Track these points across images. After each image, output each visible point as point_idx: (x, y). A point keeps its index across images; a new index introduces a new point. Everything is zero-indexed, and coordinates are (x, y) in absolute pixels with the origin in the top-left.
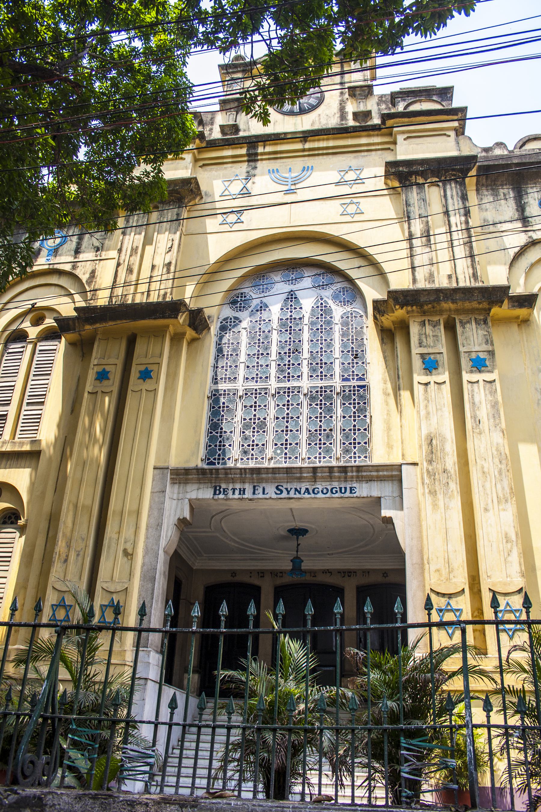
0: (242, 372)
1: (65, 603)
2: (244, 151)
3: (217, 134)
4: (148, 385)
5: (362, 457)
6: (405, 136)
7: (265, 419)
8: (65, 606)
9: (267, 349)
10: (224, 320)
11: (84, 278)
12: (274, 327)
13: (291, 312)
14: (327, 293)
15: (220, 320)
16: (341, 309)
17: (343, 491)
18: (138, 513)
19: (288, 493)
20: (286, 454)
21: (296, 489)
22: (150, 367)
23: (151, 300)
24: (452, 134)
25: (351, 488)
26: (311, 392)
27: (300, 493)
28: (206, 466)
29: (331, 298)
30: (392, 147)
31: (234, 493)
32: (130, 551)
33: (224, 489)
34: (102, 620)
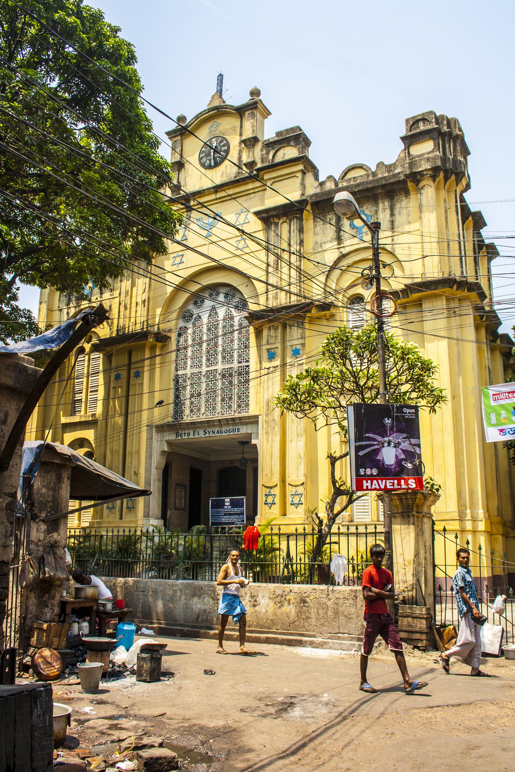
4: (138, 381)
18: (138, 452)
24: (299, 175)
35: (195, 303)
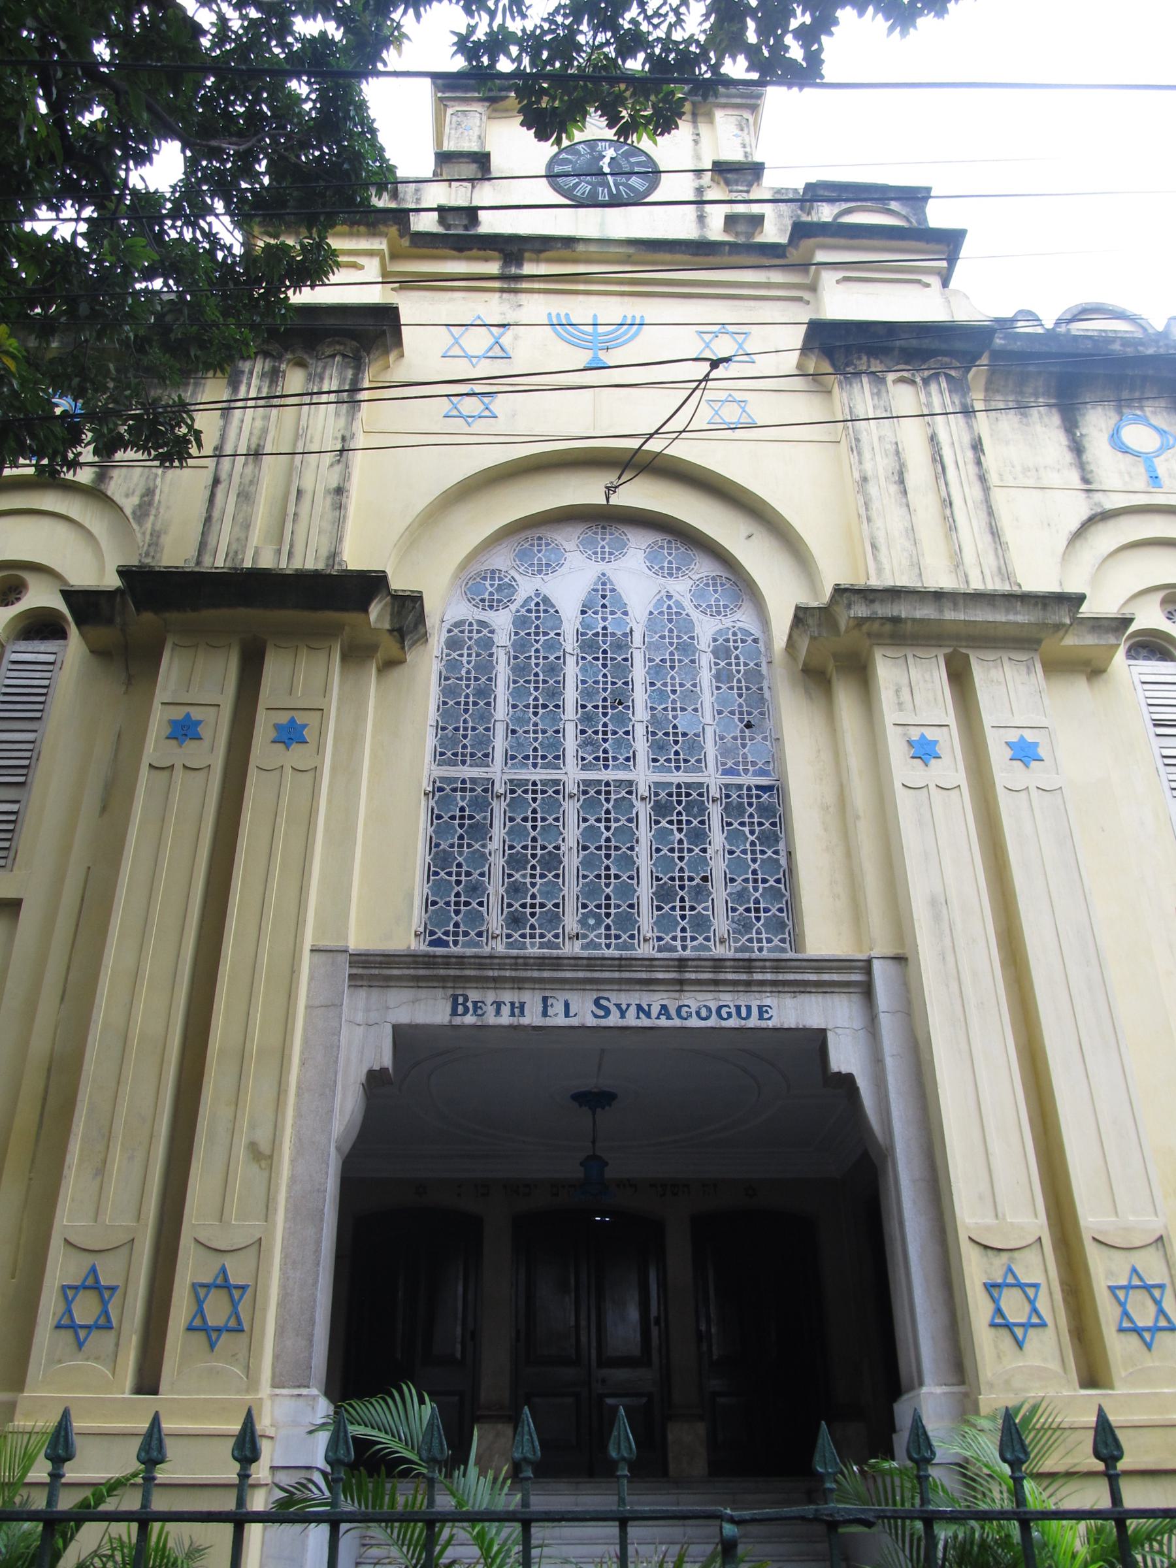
0: (500, 744)
1: (97, 1280)
2: (494, 268)
3: (426, 223)
4: (297, 755)
5: (776, 941)
6: (840, 275)
7: (557, 848)
8: (97, 1288)
9: (553, 694)
10: (457, 625)
11: (129, 505)
12: (569, 649)
13: (604, 619)
14: (680, 588)
15: (446, 626)
16: (712, 619)
17: (744, 1013)
19: (623, 1016)
20: (608, 928)
21: (639, 1008)
22: (300, 719)
23: (297, 564)
24: (935, 281)
25: (760, 1007)
26: (657, 794)
27: (648, 1015)
28: (424, 948)
29: (689, 596)
30: (806, 295)
31: (498, 1012)
32: (265, 1147)
33: (475, 1003)
34: (197, 1322)
35: (523, 555)
